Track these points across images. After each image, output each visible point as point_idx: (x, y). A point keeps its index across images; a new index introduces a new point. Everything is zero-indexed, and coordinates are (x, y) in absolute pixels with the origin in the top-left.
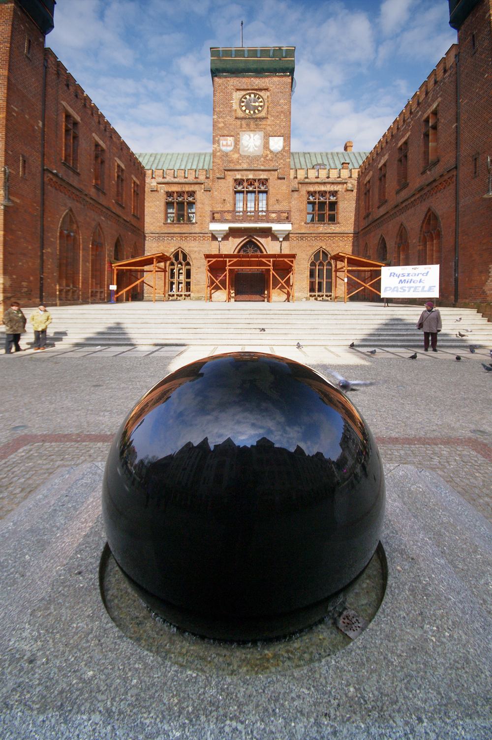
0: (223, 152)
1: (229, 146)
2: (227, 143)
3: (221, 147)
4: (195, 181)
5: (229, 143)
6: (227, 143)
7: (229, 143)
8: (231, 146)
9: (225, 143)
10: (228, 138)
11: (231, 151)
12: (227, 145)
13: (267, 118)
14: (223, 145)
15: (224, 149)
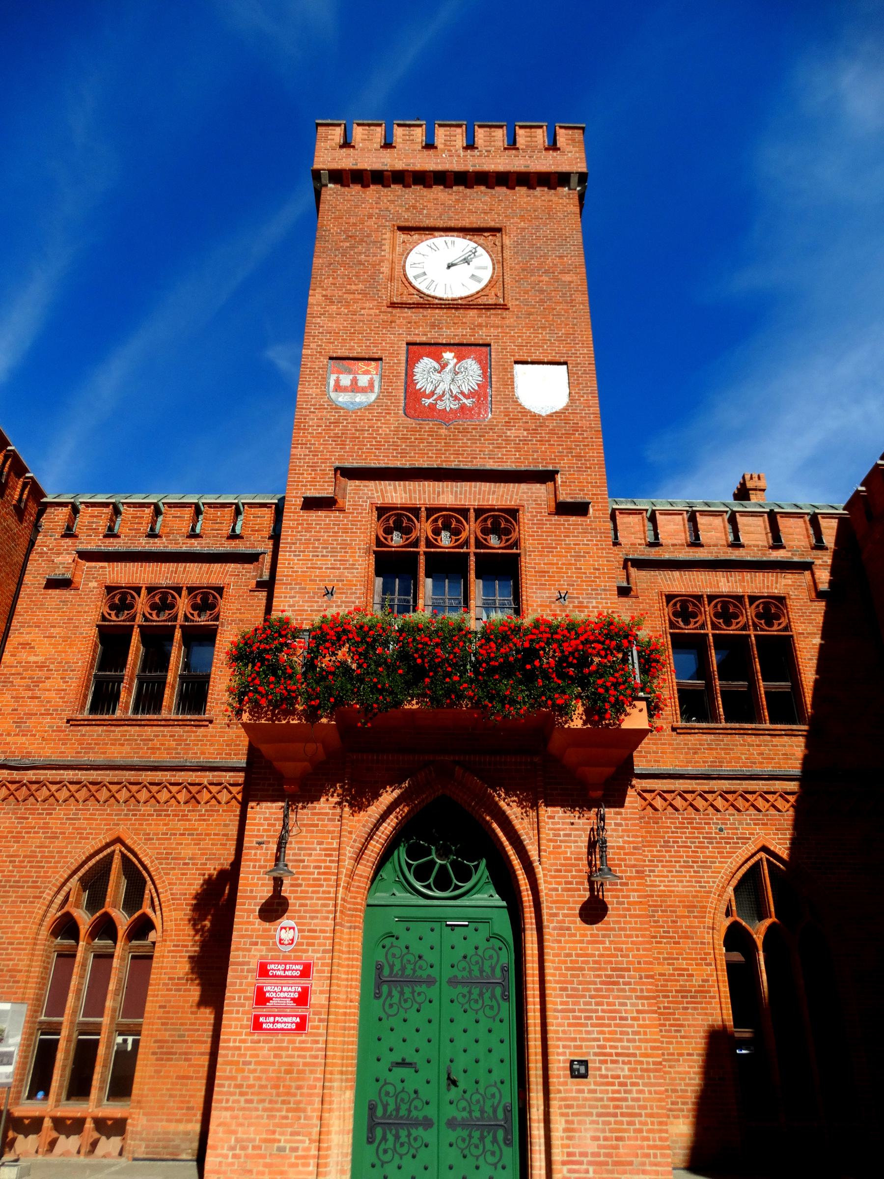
0: (337, 408)
1: (363, 390)
2: (355, 381)
3: (333, 395)
4: (229, 547)
5: (363, 380)
6: (355, 381)
7: (363, 380)
8: (372, 391)
9: (346, 380)
10: (361, 364)
11: (370, 407)
12: (354, 388)
13: (504, 307)
14: (338, 388)
15: (342, 399)
